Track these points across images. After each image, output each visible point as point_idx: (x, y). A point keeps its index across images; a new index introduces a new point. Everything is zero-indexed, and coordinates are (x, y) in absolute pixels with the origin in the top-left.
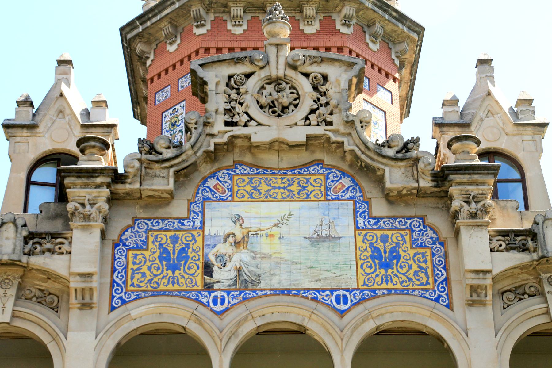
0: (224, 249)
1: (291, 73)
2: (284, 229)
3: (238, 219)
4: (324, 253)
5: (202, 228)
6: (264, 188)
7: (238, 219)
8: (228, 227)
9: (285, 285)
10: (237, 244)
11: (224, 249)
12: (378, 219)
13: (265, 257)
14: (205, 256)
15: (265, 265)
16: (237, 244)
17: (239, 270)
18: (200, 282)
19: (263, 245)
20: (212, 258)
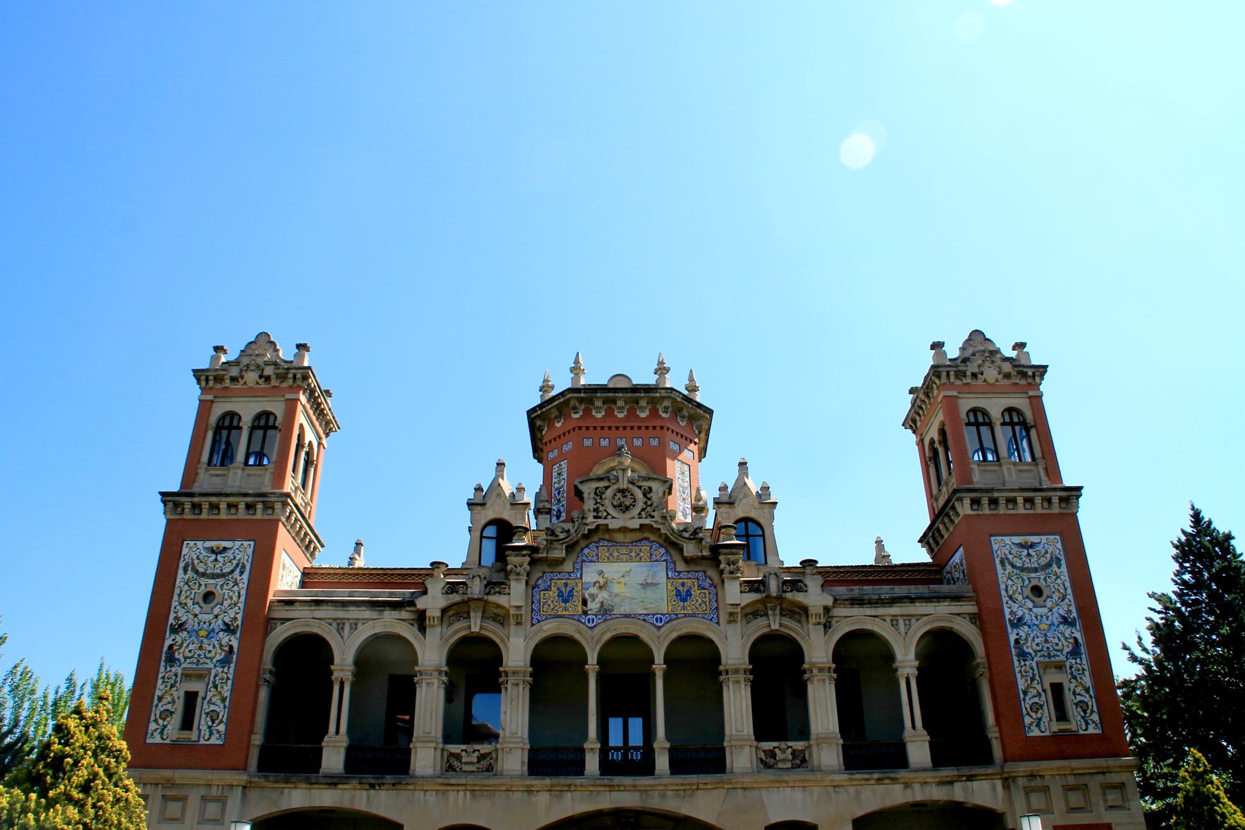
0: (594, 590)
1: (631, 486)
2: (627, 578)
3: (601, 573)
4: (649, 592)
6: (616, 554)
7: (601, 573)
8: (596, 578)
9: (628, 612)
10: (601, 588)
11: (594, 590)
12: (680, 573)
13: (617, 595)
15: (617, 600)
16: (601, 588)
17: (602, 603)
19: (616, 589)
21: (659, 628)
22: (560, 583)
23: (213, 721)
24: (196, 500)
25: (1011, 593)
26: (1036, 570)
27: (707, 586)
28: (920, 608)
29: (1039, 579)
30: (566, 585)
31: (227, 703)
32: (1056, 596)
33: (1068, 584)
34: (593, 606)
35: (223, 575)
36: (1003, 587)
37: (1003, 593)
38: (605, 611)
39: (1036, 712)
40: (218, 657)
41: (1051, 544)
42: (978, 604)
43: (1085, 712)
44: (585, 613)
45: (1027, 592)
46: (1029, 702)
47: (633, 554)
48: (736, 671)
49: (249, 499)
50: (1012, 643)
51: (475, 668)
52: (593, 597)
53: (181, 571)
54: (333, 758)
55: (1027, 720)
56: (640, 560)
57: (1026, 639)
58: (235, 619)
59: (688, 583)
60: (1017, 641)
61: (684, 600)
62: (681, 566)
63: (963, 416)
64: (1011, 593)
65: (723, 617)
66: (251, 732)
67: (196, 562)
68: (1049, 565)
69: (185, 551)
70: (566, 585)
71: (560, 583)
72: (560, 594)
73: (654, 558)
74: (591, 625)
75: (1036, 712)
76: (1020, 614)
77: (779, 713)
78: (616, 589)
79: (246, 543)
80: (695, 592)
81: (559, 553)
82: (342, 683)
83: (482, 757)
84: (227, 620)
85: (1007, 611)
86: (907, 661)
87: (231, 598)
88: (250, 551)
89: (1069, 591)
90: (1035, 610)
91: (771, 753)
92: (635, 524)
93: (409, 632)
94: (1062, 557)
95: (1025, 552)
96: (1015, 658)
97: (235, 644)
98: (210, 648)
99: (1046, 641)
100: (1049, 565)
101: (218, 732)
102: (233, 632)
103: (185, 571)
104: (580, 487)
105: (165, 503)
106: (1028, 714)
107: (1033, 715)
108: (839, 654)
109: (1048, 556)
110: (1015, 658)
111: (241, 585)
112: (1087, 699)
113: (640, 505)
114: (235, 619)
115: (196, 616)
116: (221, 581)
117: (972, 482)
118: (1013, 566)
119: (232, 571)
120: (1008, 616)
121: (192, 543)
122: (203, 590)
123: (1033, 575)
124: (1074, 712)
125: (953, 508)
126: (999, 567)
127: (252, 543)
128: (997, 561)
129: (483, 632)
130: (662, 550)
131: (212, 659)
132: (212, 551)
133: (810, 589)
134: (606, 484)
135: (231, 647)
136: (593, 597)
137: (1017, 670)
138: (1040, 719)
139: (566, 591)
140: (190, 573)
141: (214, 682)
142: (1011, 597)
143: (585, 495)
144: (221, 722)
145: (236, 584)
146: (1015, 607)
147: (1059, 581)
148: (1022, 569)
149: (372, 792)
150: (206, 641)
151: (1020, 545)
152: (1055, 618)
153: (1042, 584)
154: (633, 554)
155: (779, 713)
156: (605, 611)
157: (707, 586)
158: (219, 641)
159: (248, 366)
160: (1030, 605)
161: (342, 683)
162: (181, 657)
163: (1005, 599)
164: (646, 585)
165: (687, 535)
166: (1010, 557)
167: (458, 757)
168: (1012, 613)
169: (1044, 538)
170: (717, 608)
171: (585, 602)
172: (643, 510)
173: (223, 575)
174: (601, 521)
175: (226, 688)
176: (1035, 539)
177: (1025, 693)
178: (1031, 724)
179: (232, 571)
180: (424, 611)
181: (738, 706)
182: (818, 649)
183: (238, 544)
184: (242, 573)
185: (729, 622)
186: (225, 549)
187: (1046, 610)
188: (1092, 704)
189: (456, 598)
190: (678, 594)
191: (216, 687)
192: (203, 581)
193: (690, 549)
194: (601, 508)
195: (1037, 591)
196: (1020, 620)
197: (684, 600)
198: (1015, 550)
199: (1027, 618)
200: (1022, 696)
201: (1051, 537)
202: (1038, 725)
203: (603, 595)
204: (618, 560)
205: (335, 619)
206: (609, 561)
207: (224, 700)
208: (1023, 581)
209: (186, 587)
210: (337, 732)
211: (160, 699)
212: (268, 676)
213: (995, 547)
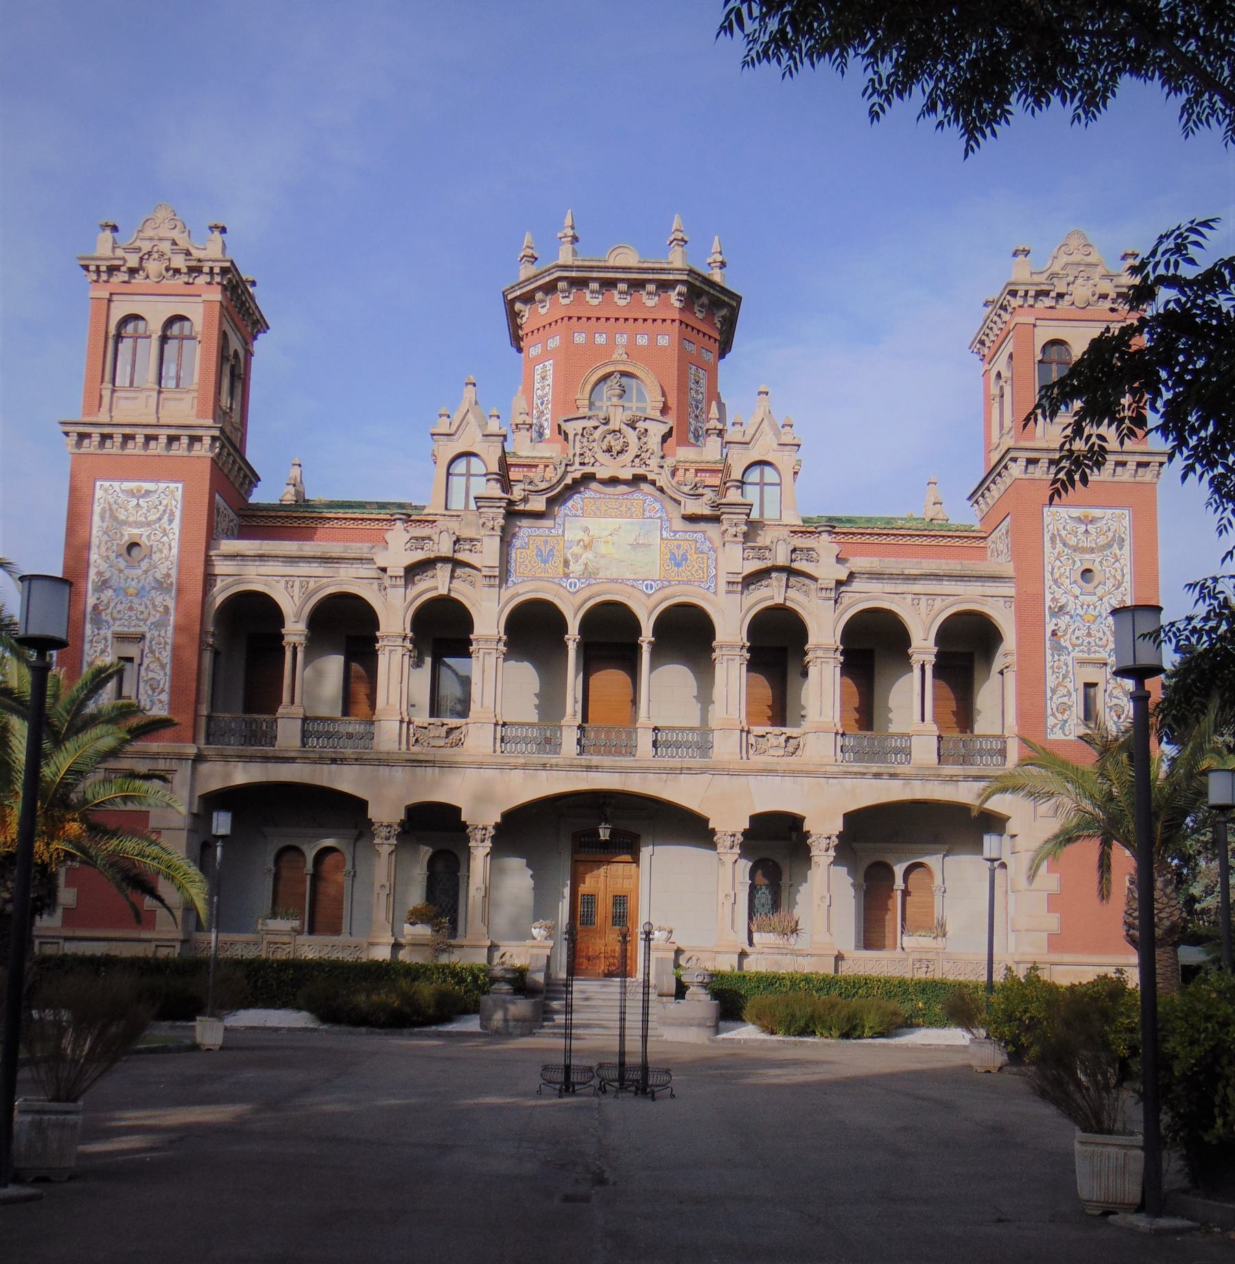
0: (577, 550)
1: (624, 427)
2: (616, 537)
3: (586, 530)
5: (563, 535)
7: (586, 530)
8: (580, 535)
9: (615, 576)
10: (585, 547)
11: (577, 550)
12: (675, 532)
13: (603, 556)
14: (565, 555)
16: (585, 547)
18: (561, 572)
20: (569, 556)
21: (649, 596)
22: (540, 541)
23: (153, 690)
25: (1057, 576)
26: (1092, 551)
27: (706, 549)
28: (947, 587)
29: (1089, 560)
30: (546, 542)
31: (168, 670)
32: (1110, 583)
33: (1127, 570)
34: (577, 568)
35: (148, 524)
36: (1048, 568)
37: (1048, 576)
38: (589, 574)
39: (1063, 713)
40: (152, 619)
43: (1119, 717)
44: (567, 576)
46: (1057, 700)
47: (623, 509)
48: (732, 647)
49: (173, 432)
50: (1048, 634)
52: (577, 557)
54: (288, 733)
55: (1051, 721)
56: (631, 517)
57: (1065, 631)
58: (168, 576)
59: (685, 545)
60: (1054, 633)
61: (678, 565)
62: (679, 524)
64: (1057, 576)
65: (722, 586)
66: (198, 702)
68: (1109, 545)
69: (99, 493)
70: (546, 542)
71: (540, 541)
72: (540, 553)
73: (647, 514)
75: (1063, 713)
76: (1063, 601)
78: (603, 549)
79: (172, 486)
80: (693, 557)
81: (538, 504)
82: (295, 648)
83: (450, 731)
84: (158, 576)
85: (1048, 597)
86: (924, 647)
87: (161, 551)
88: (179, 494)
89: (1128, 578)
90: (1081, 598)
92: (627, 474)
94: (1127, 538)
97: (171, 604)
98: (142, 608)
99: (1089, 635)
100: (1109, 545)
101: (161, 702)
102: (168, 590)
104: (565, 426)
106: (1053, 715)
107: (1059, 716)
109: (1110, 534)
110: (1048, 652)
111: (171, 536)
113: (633, 450)
114: (168, 576)
115: (121, 571)
118: (1065, 545)
119: (160, 519)
120: (1048, 603)
121: (107, 484)
123: (1087, 556)
126: (1047, 544)
127: (180, 485)
128: (1047, 538)
130: (657, 506)
131: (145, 620)
132: (131, 493)
133: (822, 559)
134: (597, 424)
135: (167, 608)
136: (577, 557)
137: (1049, 665)
138: (1066, 721)
139: (545, 550)
141: (150, 647)
142: (1056, 581)
144: (163, 691)
145: (165, 533)
146: (1059, 593)
148: (1076, 549)
149: (334, 766)
150: (136, 600)
151: (1079, 520)
153: (1096, 567)
154: (623, 509)
157: (706, 549)
158: (152, 601)
160: (1077, 591)
161: (295, 648)
163: (1048, 582)
164: (635, 546)
165: (686, 489)
166: (1063, 533)
168: (1053, 599)
169: (1110, 511)
170: (716, 575)
171: (566, 563)
172: (637, 456)
173: (148, 524)
174: (588, 469)
175: (164, 654)
176: (1096, 512)
177: (1054, 691)
178: (1054, 726)
179: (160, 519)
180: (384, 570)
183: (162, 485)
184: (171, 521)
185: (728, 592)
186: (148, 493)
187: (1095, 598)
189: (420, 556)
190: (673, 557)
191: (152, 652)
194: (588, 453)
196: (1061, 608)
197: (678, 565)
200: (1049, 694)
201: (1118, 511)
202: (1062, 728)
203: (588, 556)
204: (606, 515)
206: (595, 516)
207: (163, 667)
208: (1074, 562)
209: (105, 538)
210: (292, 702)
212: (211, 641)
213: (1047, 520)
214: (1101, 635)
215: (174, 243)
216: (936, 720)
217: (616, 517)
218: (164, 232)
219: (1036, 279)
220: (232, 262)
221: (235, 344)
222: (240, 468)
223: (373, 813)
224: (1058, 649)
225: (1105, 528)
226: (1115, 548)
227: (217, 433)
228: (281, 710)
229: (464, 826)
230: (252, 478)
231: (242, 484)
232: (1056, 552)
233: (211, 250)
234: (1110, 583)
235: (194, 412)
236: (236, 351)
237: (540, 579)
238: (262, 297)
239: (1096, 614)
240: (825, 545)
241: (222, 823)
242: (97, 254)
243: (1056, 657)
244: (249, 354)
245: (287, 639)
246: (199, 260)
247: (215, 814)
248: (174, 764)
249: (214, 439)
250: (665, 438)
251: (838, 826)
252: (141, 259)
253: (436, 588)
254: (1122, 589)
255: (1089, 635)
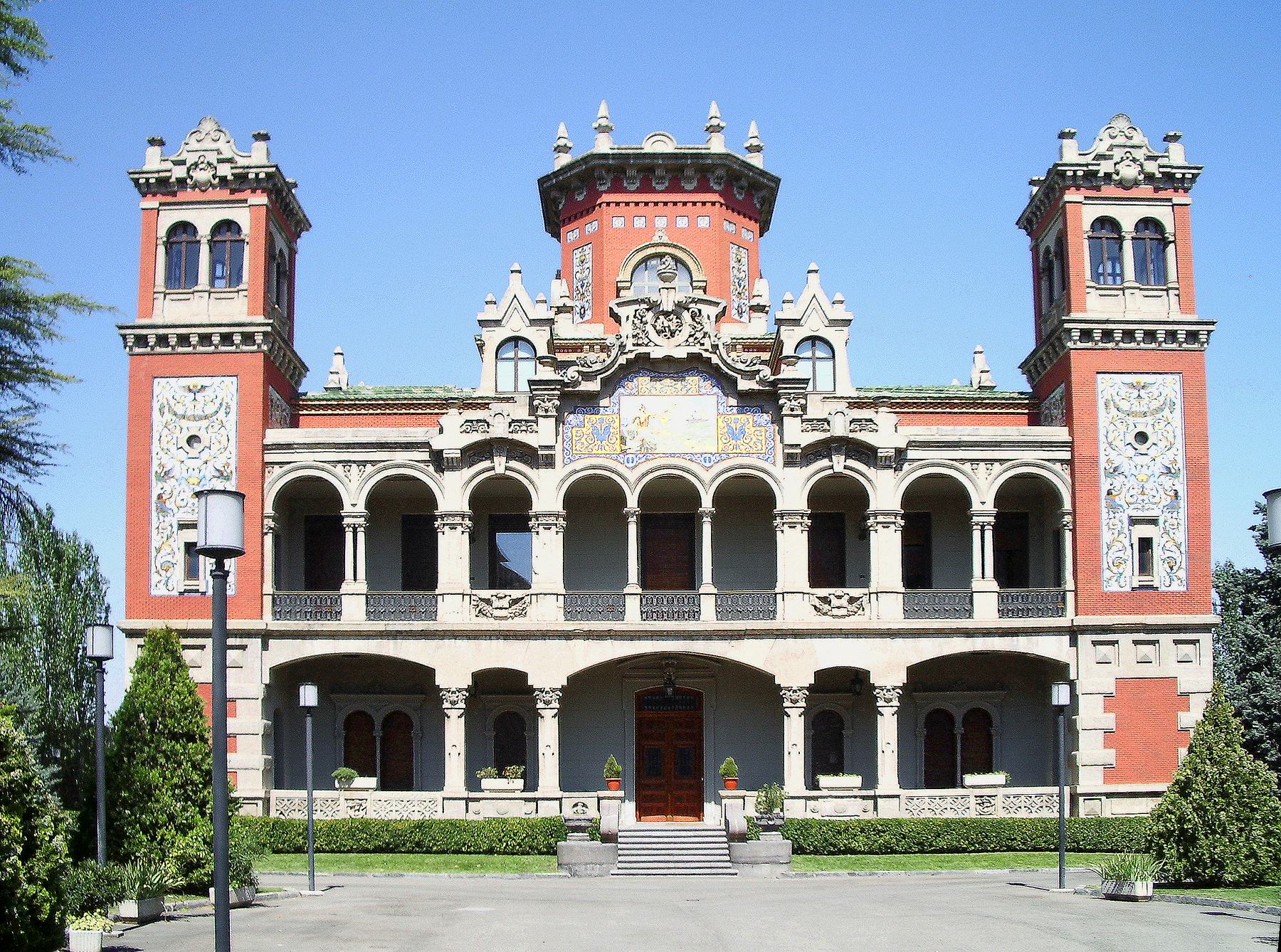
24: (161, 331)
26: (1145, 414)
32: (1161, 445)
33: (1179, 432)
34: (633, 445)
35: (206, 417)
36: (1102, 432)
37: (1102, 438)
41: (1170, 386)
42: (1072, 451)
44: (624, 452)
45: (1130, 438)
46: (1113, 554)
50: (1104, 494)
51: (500, 512)
53: (156, 413)
55: (1107, 574)
58: (228, 465)
63: (1086, 226)
65: (780, 460)
67: (172, 402)
68: (1160, 409)
74: (630, 465)
77: (836, 560)
81: (594, 386)
83: (515, 601)
91: (825, 600)
93: (427, 476)
95: (1136, 393)
96: (1104, 511)
99: (1143, 493)
100: (1160, 409)
103: (162, 414)
104: (616, 310)
105: (124, 337)
106: (1109, 568)
108: (909, 498)
109: (1162, 399)
112: (1176, 555)
116: (205, 423)
117: (1085, 310)
122: (186, 435)
124: (1159, 568)
125: (1059, 339)
129: (508, 473)
137: (1104, 522)
140: (168, 416)
142: (1110, 444)
143: (624, 319)
146: (1113, 455)
147: (1169, 427)
152: (1158, 468)
155: (836, 560)
156: (647, 452)
159: (196, 165)
160: (1131, 452)
162: (173, 506)
166: (1117, 399)
167: (488, 602)
171: (623, 440)
173: (206, 417)
181: (793, 549)
182: (886, 492)
188: (1182, 560)
192: (184, 423)
193: (744, 385)
195: (1142, 437)
198: (1124, 391)
199: (1125, 468)
200: (1105, 550)
203: (644, 432)
205: (340, 462)
211: (158, 550)
212: (272, 524)
213: (1100, 387)
214: (1154, 493)
215: (219, 152)
216: (997, 576)
217: (671, 395)
218: (208, 144)
219: (1083, 160)
220: (276, 166)
221: (280, 244)
222: (290, 361)
223: (440, 681)
224: (1113, 508)
225: (1156, 393)
226: (1166, 412)
227: (269, 329)
228: (345, 588)
229: (531, 690)
230: (300, 369)
231: (291, 377)
232: (1110, 416)
233: (257, 157)
234: (1161, 445)
235: (245, 309)
236: (281, 251)
237: (597, 456)
238: (305, 199)
239: (1149, 473)
240: (884, 418)
241: (309, 695)
242: (145, 168)
243: (1112, 515)
244: (293, 252)
245: (346, 521)
246: (243, 168)
247: (302, 688)
248: (245, 641)
249: (265, 334)
250: (718, 318)
251: (901, 678)
252: (189, 170)
253: (493, 468)
254: (1173, 450)
255: (1143, 493)
